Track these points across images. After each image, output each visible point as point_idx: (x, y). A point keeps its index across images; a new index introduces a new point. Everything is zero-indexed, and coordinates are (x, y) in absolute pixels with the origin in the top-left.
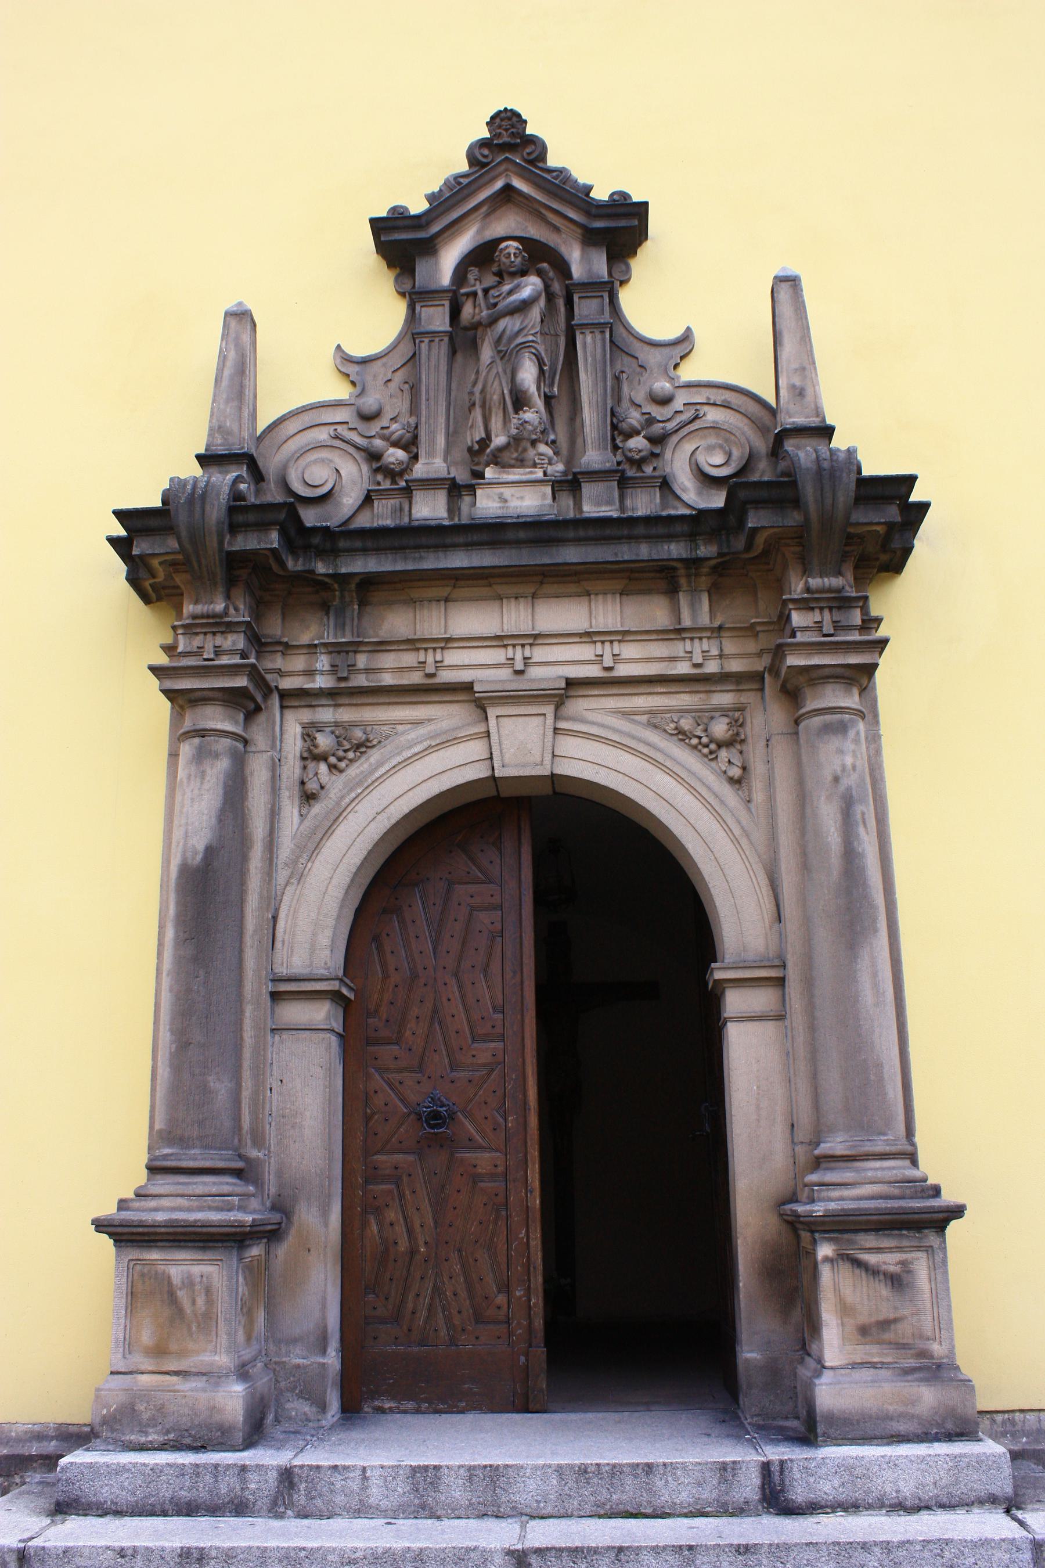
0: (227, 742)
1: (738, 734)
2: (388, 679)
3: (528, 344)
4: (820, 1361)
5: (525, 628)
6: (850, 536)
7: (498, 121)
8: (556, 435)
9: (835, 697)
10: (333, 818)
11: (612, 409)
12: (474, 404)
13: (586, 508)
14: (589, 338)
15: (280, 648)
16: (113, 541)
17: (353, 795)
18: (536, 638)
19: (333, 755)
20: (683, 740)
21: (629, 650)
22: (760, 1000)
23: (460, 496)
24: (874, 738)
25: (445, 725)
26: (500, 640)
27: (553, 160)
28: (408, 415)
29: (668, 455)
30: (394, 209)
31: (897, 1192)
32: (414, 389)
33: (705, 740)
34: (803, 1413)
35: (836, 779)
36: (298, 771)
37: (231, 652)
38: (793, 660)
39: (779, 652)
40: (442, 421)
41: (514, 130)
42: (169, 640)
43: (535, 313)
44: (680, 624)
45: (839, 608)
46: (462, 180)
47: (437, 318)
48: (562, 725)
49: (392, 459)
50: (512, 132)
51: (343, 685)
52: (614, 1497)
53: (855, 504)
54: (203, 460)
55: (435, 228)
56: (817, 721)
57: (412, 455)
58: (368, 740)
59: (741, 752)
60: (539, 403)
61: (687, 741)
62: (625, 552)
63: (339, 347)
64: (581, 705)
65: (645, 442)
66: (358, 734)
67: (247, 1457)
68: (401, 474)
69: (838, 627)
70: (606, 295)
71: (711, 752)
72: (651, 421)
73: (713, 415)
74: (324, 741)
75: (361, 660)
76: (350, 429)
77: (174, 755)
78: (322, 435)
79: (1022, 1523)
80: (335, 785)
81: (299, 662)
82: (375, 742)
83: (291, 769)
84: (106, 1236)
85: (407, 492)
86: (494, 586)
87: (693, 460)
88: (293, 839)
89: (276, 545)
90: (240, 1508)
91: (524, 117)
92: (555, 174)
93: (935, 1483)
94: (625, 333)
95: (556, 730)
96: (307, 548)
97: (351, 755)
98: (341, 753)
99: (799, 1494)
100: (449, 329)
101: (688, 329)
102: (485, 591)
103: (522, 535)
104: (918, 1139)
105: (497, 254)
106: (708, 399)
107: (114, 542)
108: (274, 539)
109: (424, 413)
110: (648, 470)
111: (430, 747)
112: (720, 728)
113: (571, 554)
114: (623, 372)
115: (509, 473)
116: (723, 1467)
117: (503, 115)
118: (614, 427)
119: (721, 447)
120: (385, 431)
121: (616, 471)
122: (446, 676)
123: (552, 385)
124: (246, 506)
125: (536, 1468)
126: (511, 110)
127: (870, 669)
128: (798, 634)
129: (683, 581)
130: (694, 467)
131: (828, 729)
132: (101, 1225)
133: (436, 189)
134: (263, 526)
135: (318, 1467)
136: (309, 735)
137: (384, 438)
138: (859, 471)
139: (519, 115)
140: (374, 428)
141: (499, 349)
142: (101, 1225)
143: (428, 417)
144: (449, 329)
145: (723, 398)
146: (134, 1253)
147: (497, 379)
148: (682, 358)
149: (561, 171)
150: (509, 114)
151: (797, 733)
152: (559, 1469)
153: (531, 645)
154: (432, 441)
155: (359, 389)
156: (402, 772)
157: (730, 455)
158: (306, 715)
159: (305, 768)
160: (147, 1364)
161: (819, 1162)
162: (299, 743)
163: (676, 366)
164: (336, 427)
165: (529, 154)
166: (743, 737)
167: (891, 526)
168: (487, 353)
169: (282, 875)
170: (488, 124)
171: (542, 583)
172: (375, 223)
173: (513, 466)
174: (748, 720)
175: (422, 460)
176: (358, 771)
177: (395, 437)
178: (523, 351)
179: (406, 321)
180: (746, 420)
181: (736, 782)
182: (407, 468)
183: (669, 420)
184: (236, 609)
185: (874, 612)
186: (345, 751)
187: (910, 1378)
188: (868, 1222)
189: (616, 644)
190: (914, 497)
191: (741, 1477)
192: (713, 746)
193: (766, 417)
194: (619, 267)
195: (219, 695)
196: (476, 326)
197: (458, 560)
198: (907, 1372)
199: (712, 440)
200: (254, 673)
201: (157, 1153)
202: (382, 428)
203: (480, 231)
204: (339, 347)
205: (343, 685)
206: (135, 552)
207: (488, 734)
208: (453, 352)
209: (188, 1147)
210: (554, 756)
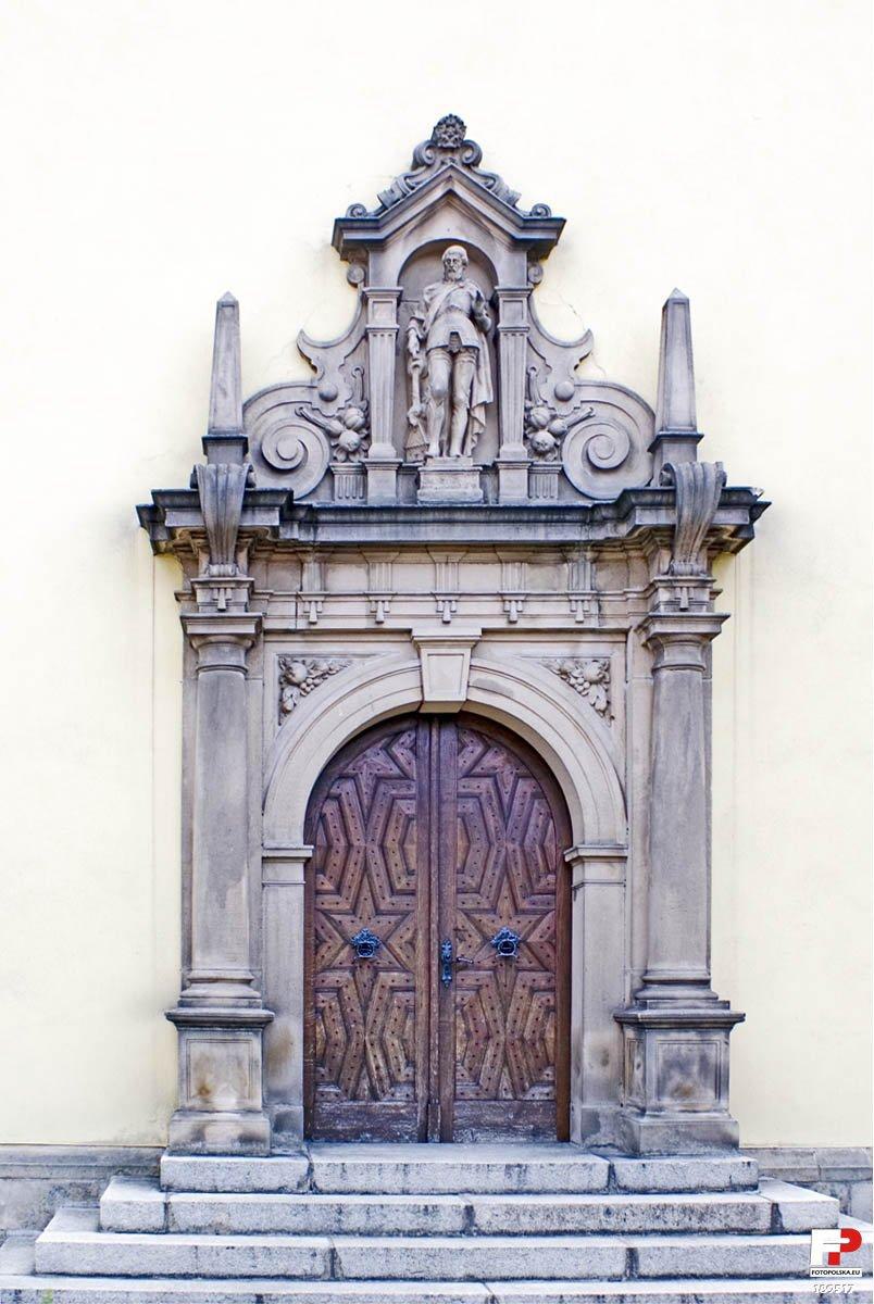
1: (604, 677)
15: (267, 597)
19: (305, 682)
20: (565, 680)
27: (483, 167)
29: (565, 446)
30: (353, 208)
33: (581, 680)
41: (457, 136)
42: (180, 589)
48: (473, 663)
57: (363, 436)
58: (330, 669)
59: (606, 691)
66: (324, 666)
76: (314, 409)
86: (432, 554)
97: (317, 681)
98: (310, 681)
101: (589, 331)
107: (140, 509)
108: (273, 519)
112: (593, 671)
117: (448, 122)
122: (389, 624)
124: (254, 492)
126: (456, 117)
132: (170, 1017)
133: (388, 188)
137: (340, 419)
140: (331, 409)
148: (581, 360)
150: (454, 121)
159: (282, 689)
161: (646, 983)
163: (576, 367)
165: (467, 159)
172: (338, 221)
185: (716, 586)
192: (587, 685)
195: (233, 639)
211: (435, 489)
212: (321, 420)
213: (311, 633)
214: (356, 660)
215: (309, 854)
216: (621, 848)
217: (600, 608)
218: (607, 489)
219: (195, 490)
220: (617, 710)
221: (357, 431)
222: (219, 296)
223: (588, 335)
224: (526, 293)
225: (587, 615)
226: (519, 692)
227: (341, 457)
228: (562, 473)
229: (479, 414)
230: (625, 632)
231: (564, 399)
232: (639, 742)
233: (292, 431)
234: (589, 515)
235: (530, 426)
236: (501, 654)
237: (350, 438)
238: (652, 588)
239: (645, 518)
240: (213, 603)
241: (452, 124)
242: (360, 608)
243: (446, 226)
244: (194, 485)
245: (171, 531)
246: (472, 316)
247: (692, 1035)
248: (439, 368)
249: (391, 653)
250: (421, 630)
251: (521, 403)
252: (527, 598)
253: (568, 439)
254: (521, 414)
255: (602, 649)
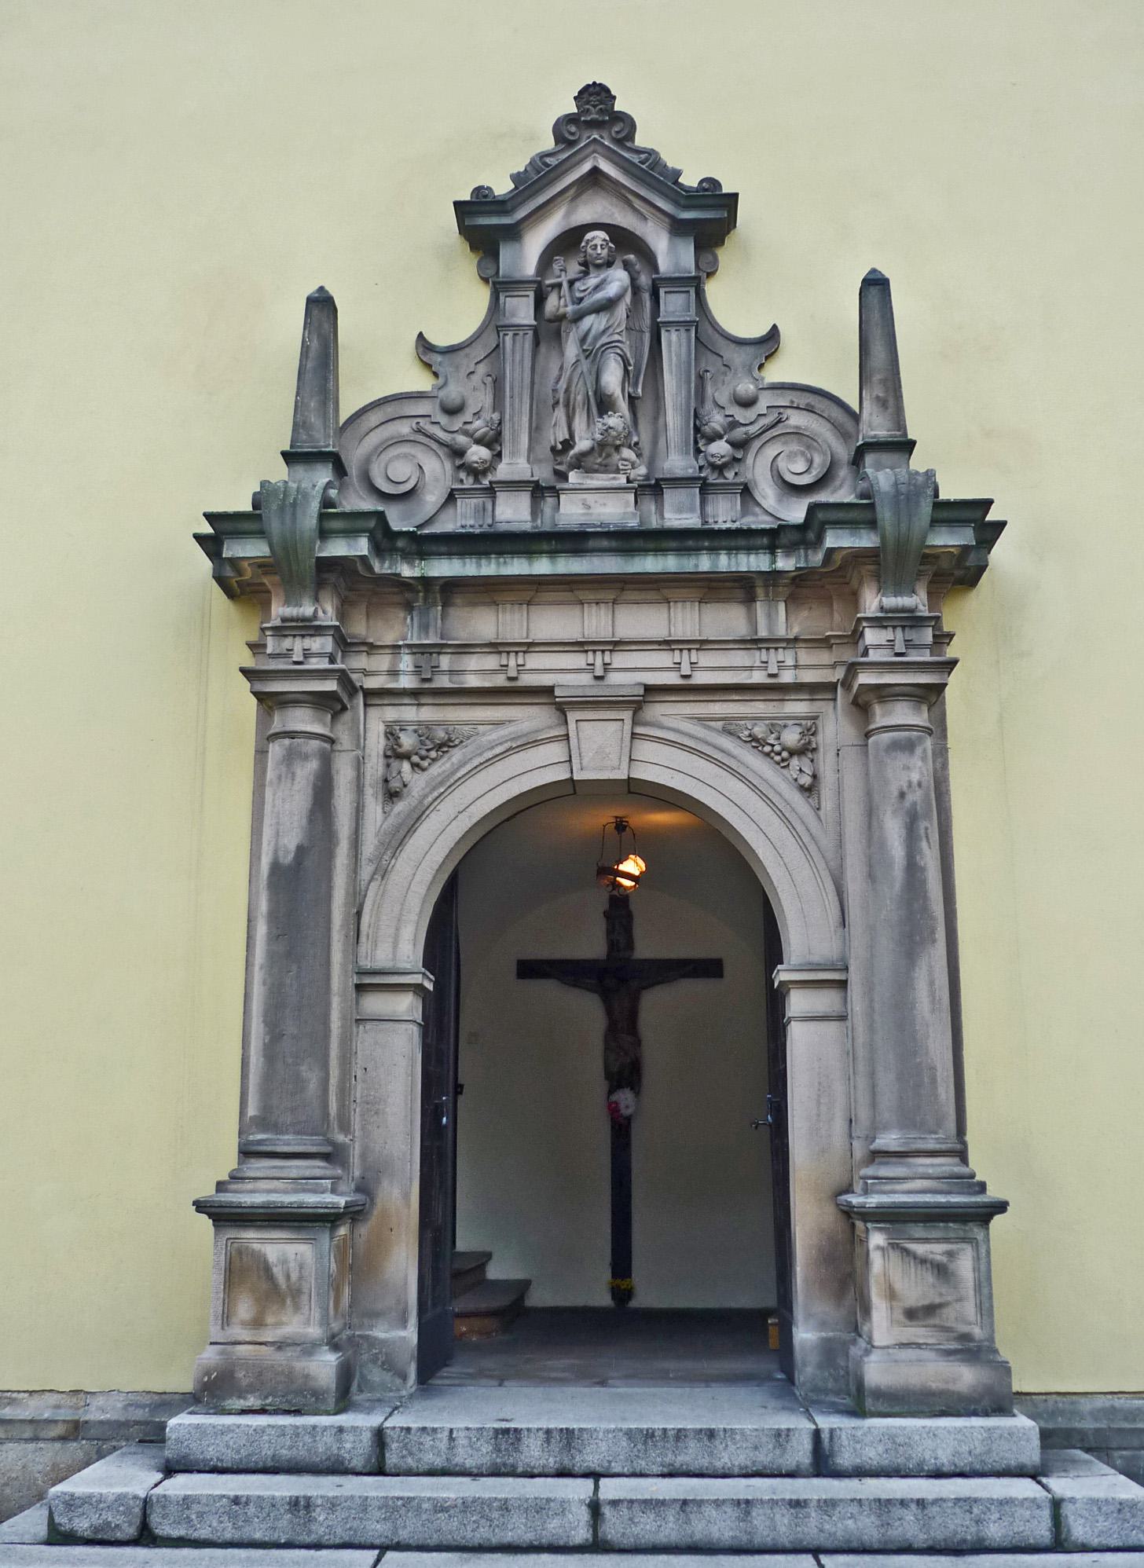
0: (315, 744)
1: (810, 743)
2: (473, 681)
3: (613, 345)
4: (870, 1342)
5: (605, 634)
6: (925, 556)
7: (585, 95)
8: (639, 436)
9: (903, 714)
10: (416, 816)
11: (695, 410)
12: (557, 403)
13: (667, 515)
14: (674, 336)
15: (365, 649)
16: (199, 538)
17: (436, 794)
18: (616, 645)
19: (416, 754)
21: (706, 659)
22: (824, 1001)
23: (543, 497)
24: (941, 753)
25: (525, 726)
26: (580, 646)
27: (641, 140)
28: (491, 410)
29: (750, 460)
30: (478, 191)
31: (944, 1187)
32: (498, 385)
33: (777, 748)
34: (853, 1389)
35: (902, 795)
36: (381, 770)
37: (320, 655)
38: (865, 678)
39: (852, 669)
40: (525, 419)
42: (254, 637)
43: (621, 310)
44: (756, 634)
45: (911, 627)
46: (548, 160)
47: (521, 310)
48: (639, 730)
49: (475, 458)
50: (601, 109)
51: (426, 686)
52: (680, 1458)
53: (931, 526)
54: (289, 457)
55: (521, 214)
56: (886, 737)
57: (495, 453)
58: (450, 740)
59: (812, 761)
60: (623, 405)
61: (760, 748)
62: (704, 563)
63: (421, 335)
64: (660, 711)
65: (729, 447)
66: (441, 734)
67: (343, 1419)
68: (484, 472)
69: (909, 645)
70: (692, 291)
71: (783, 760)
72: (734, 424)
73: (796, 419)
74: (407, 741)
75: (445, 662)
77: (261, 753)
78: (404, 428)
79: (1044, 1486)
80: (417, 783)
81: (383, 662)
82: (457, 742)
83: (375, 767)
84: (205, 1216)
85: (491, 491)
86: (577, 593)
87: (775, 466)
88: (377, 835)
89: (365, 552)
90: (336, 1468)
91: (613, 93)
92: (643, 156)
93: (970, 1452)
94: (710, 331)
95: (634, 735)
96: (393, 550)
97: (433, 754)
98: (424, 753)
99: (845, 1459)
100: (534, 323)
101: (775, 327)
102: (568, 595)
103: (605, 543)
104: (969, 1138)
105: (583, 244)
106: (792, 402)
108: (362, 547)
109: (508, 411)
110: (730, 475)
111: (511, 749)
112: (791, 737)
113: (649, 564)
114: (707, 371)
115: (592, 478)
116: (778, 1434)
117: (591, 89)
118: (697, 430)
119: (803, 454)
120: (468, 427)
121: (699, 478)
122: (527, 680)
123: (636, 385)
125: (608, 1431)
126: (600, 84)
127: (940, 688)
128: (871, 652)
129: (760, 592)
130: (775, 472)
131: (895, 746)
132: (200, 1206)
133: (522, 169)
134: (351, 533)
135: (408, 1430)
136: (392, 734)
137: (466, 433)
138: (936, 494)
139: (608, 91)
140: (457, 423)
141: (585, 348)
142: (200, 1206)
143: (512, 417)
144: (534, 323)
145: (807, 401)
146: (232, 1233)
147: (581, 379)
148: (767, 358)
149: (651, 153)
150: (597, 88)
151: (867, 745)
152: (629, 1434)
153: (611, 651)
154: (515, 440)
155: (441, 381)
156: (483, 773)
157: (811, 462)
158: (391, 714)
159: (388, 766)
160: (245, 1335)
162: (382, 741)
163: (761, 367)
164: (418, 420)
165: (617, 132)
166: (814, 746)
167: (965, 549)
168: (572, 350)
169: (366, 871)
170: (575, 98)
171: (623, 589)
173: (596, 471)
174: (820, 729)
175: (505, 460)
176: (440, 770)
177: (478, 434)
178: (609, 350)
179: (489, 309)
180: (829, 425)
182: (489, 468)
183: (751, 423)
184: (324, 612)
186: (428, 750)
187: (951, 1358)
188: (917, 1214)
189: (694, 652)
190: (991, 517)
191: (794, 1442)
192: (785, 754)
193: (849, 424)
194: (707, 257)
195: (306, 698)
196: (561, 318)
197: (542, 566)
198: (949, 1353)
199: (795, 447)
200: (343, 677)
201: (251, 1138)
202: (465, 423)
203: (567, 215)
204: (421, 335)
205: (426, 686)
206: (227, 553)
207: (567, 737)
208: (537, 343)
209: (282, 1133)
210: (631, 760)
219: (258, 512)
222: (311, 289)
224: (694, 284)
230: (831, 687)
233: (405, 449)
234: (775, 538)
241: (595, 95)
243: (594, 209)
244: (255, 506)
245: (234, 562)
249: (529, 718)
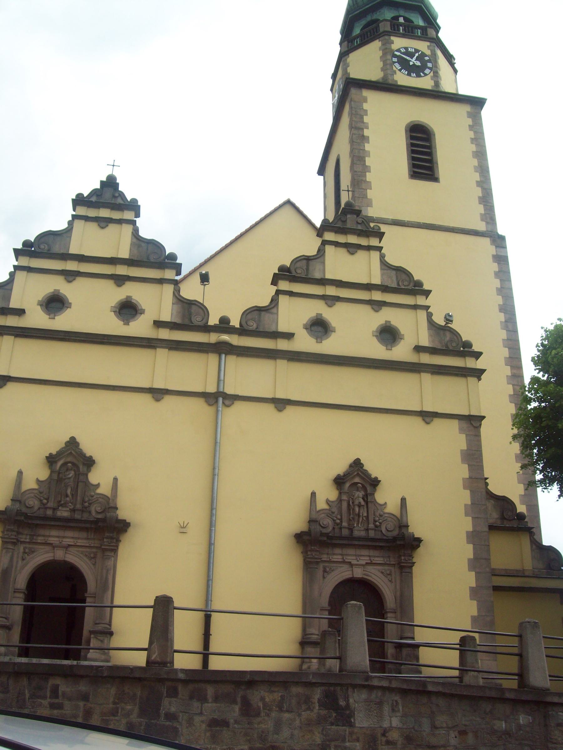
48: (364, 569)
112: (388, 572)
122: (346, 560)
140: (334, 515)
181: (390, 581)
211: (356, 533)
212: (332, 517)
213: (330, 562)
214: (339, 568)
215: (329, 609)
216: (395, 610)
217: (390, 559)
218: (390, 535)
220: (393, 580)
221: (339, 520)
223: (386, 503)
224: (373, 494)
225: (387, 561)
226: (373, 576)
227: (336, 525)
228: (381, 531)
229: (364, 518)
230: (394, 565)
231: (381, 516)
232: (398, 587)
234: (387, 541)
235: (375, 521)
236: (370, 568)
237: (338, 521)
238: (400, 556)
239: (398, 543)
240: (312, 554)
242: (340, 557)
243: (357, 480)
246: (363, 499)
247: (411, 649)
248: (357, 509)
249: (345, 567)
250: (354, 562)
251: (373, 516)
252: (375, 557)
253: (382, 524)
254: (373, 519)
255: (390, 568)
